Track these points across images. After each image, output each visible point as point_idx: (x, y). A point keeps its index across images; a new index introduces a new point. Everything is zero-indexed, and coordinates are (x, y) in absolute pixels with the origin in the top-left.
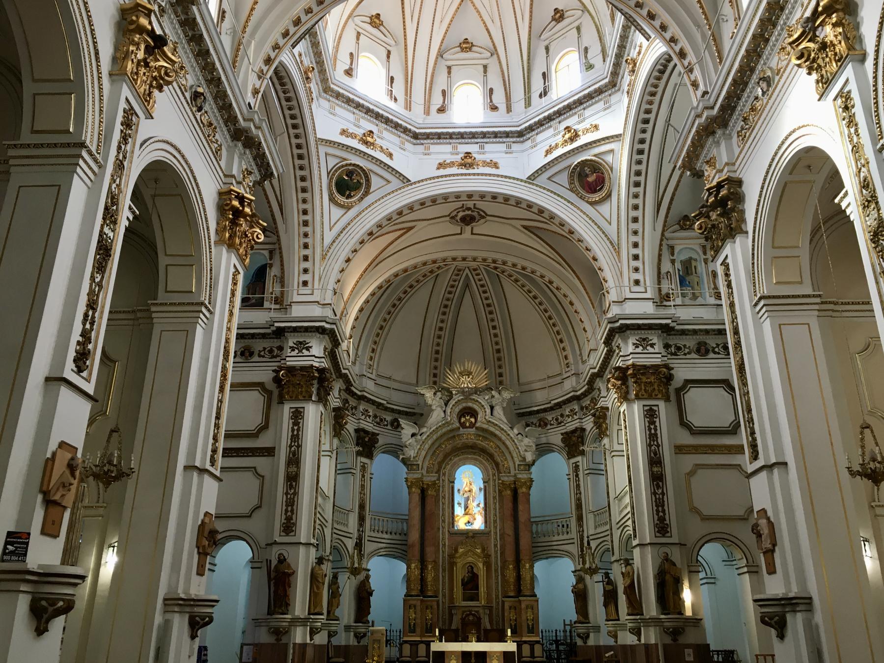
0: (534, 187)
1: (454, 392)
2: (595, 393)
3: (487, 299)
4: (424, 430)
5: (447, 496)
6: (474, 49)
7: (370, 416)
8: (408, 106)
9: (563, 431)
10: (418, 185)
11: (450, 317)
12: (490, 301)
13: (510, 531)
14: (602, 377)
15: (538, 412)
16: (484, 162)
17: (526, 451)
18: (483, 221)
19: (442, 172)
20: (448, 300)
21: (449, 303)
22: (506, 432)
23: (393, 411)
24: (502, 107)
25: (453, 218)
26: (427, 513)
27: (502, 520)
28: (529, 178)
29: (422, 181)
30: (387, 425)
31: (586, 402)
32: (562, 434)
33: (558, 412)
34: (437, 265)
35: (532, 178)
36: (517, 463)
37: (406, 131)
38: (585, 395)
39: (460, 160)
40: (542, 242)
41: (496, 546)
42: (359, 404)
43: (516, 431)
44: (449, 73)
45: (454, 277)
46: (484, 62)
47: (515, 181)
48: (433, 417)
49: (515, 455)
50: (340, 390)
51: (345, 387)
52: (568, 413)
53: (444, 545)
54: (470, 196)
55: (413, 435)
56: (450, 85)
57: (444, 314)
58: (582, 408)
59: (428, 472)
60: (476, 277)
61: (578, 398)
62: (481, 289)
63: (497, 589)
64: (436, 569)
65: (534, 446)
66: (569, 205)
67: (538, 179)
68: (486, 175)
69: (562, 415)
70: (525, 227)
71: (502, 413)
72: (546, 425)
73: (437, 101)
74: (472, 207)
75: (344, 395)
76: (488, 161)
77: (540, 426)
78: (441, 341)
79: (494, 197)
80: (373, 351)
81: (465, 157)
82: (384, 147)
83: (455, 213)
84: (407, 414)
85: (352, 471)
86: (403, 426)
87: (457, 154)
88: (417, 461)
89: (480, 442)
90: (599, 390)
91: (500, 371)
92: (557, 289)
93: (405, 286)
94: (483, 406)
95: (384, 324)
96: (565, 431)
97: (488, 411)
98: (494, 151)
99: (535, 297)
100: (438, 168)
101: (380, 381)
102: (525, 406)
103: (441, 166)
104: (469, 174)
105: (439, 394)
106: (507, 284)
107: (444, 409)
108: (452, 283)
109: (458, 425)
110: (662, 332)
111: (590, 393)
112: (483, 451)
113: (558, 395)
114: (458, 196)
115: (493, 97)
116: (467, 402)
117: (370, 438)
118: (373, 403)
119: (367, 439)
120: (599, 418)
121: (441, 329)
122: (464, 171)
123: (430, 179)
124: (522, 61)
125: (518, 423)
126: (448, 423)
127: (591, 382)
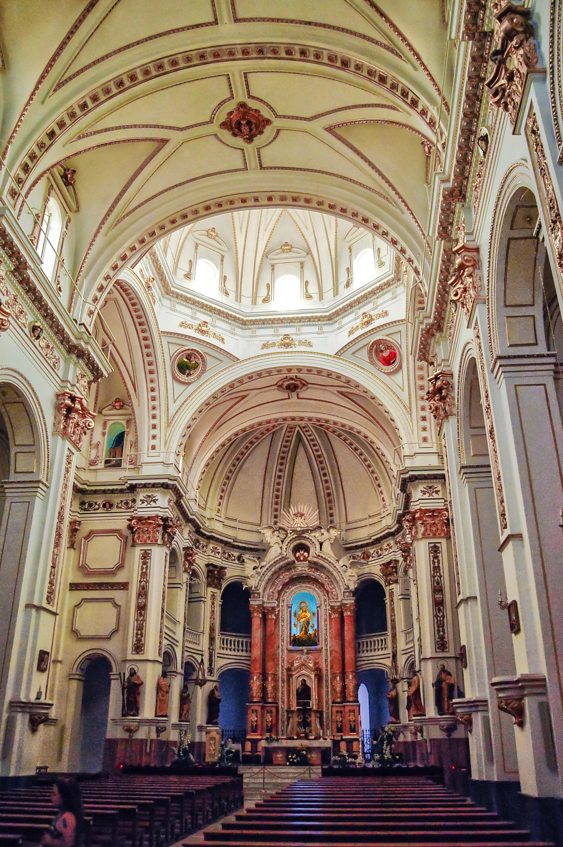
1: (289, 532)
3: (317, 451)
4: (263, 564)
5: (285, 619)
8: (238, 298)
9: (381, 563)
12: (319, 453)
15: (362, 546)
17: (349, 580)
18: (304, 388)
19: (266, 351)
20: (284, 452)
21: (285, 455)
25: (280, 386)
31: (399, 538)
37: (235, 319)
41: (326, 660)
49: (340, 583)
50: (190, 532)
51: (194, 530)
53: (283, 660)
54: (289, 370)
55: (254, 569)
56: (273, 280)
61: (392, 534)
63: (327, 695)
64: (275, 680)
69: (381, 549)
71: (329, 548)
73: (263, 292)
75: (195, 536)
77: (363, 558)
80: (221, 497)
81: (284, 338)
84: (251, 550)
85: (203, 599)
87: (278, 336)
91: (331, 511)
92: (371, 442)
93: (246, 443)
97: (318, 546)
99: (356, 449)
100: (262, 348)
101: (227, 522)
103: (265, 346)
105: (276, 532)
108: (286, 438)
109: (293, 559)
111: (401, 530)
112: (315, 581)
113: (375, 531)
114: (279, 371)
118: (221, 541)
119: (216, 573)
121: (280, 477)
122: (284, 350)
125: (344, 556)
126: (283, 558)
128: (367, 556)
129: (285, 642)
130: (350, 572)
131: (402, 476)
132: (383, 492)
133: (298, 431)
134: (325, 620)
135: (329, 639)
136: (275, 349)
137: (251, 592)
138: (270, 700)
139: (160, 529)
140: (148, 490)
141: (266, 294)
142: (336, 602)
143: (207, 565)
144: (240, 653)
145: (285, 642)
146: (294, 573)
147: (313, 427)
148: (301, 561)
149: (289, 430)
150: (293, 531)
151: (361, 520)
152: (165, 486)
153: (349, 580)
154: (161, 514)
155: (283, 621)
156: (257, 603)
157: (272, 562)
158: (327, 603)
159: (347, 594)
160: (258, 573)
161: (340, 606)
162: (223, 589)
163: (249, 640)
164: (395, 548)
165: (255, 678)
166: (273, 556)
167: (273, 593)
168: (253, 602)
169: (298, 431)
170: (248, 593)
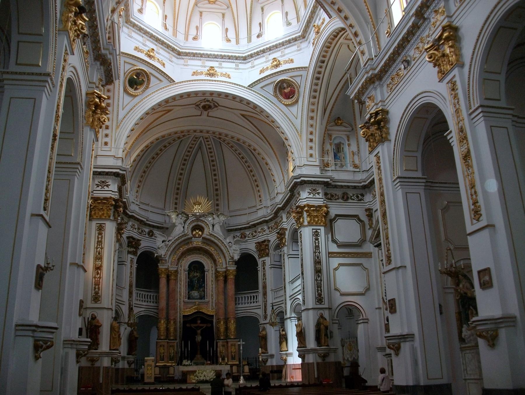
2: (278, 220)
3: (212, 157)
4: (170, 238)
5: (183, 279)
6: (217, 2)
7: (135, 229)
8: (175, 34)
10: (179, 84)
11: (188, 168)
12: (213, 158)
13: (222, 302)
14: (284, 210)
16: (222, 73)
17: (234, 253)
18: (216, 109)
20: (187, 156)
21: (188, 158)
22: (221, 241)
23: (150, 225)
24: (233, 41)
25: (197, 106)
26: (171, 290)
27: (218, 295)
28: (248, 86)
30: (145, 235)
31: (272, 224)
32: (256, 243)
34: (183, 134)
35: (251, 86)
36: (228, 260)
37: (173, 50)
38: (271, 220)
39: (206, 71)
42: (129, 221)
43: (228, 241)
44: (201, 16)
45: (192, 142)
46: (223, 11)
47: (240, 87)
48: (176, 230)
49: (226, 255)
52: (259, 231)
54: (212, 93)
55: (163, 242)
56: (201, 23)
57: (184, 165)
58: (269, 228)
59: (171, 264)
60: (206, 143)
61: (266, 222)
62: (209, 150)
66: (272, 105)
67: (254, 87)
68: (223, 82)
70: (243, 115)
72: (245, 237)
73: (193, 32)
76: (224, 73)
78: (181, 182)
79: (227, 95)
80: (139, 186)
81: (210, 69)
82: (160, 60)
84: (158, 228)
86: (157, 235)
87: (205, 67)
88: (165, 258)
89: (204, 247)
90: (281, 217)
91: (217, 202)
92: (259, 154)
95: (146, 170)
96: (257, 241)
97: (211, 228)
98: (228, 67)
99: (243, 158)
100: (193, 75)
102: (231, 226)
103: (194, 74)
105: (180, 215)
106: (226, 150)
107: (183, 225)
108: (191, 145)
109: (191, 236)
110: (324, 186)
113: (254, 218)
114: (204, 93)
115: (228, 34)
116: (198, 222)
117: (136, 242)
119: (134, 243)
120: (281, 234)
121: (181, 174)
122: (209, 78)
123: (187, 81)
124: (247, 14)
126: (185, 235)
127: (276, 214)
128: (243, 236)
129: (182, 296)
130: (234, 247)
131: (295, 180)
134: (212, 281)
135: (214, 295)
137: (160, 259)
138: (172, 338)
139: (112, 208)
140: (102, 176)
143: (128, 238)
144: (149, 304)
145: (182, 296)
146: (191, 246)
147: (213, 139)
148: (197, 237)
149: (194, 139)
150: (193, 215)
151: (239, 210)
152: (116, 175)
154: (113, 196)
155: (181, 281)
156: (164, 267)
157: (177, 237)
158: (214, 269)
159: (231, 263)
160: (166, 245)
161: (225, 272)
162: (138, 255)
163: (155, 295)
164: (267, 232)
165: (162, 322)
166: (178, 233)
167: (175, 260)
168: (161, 267)
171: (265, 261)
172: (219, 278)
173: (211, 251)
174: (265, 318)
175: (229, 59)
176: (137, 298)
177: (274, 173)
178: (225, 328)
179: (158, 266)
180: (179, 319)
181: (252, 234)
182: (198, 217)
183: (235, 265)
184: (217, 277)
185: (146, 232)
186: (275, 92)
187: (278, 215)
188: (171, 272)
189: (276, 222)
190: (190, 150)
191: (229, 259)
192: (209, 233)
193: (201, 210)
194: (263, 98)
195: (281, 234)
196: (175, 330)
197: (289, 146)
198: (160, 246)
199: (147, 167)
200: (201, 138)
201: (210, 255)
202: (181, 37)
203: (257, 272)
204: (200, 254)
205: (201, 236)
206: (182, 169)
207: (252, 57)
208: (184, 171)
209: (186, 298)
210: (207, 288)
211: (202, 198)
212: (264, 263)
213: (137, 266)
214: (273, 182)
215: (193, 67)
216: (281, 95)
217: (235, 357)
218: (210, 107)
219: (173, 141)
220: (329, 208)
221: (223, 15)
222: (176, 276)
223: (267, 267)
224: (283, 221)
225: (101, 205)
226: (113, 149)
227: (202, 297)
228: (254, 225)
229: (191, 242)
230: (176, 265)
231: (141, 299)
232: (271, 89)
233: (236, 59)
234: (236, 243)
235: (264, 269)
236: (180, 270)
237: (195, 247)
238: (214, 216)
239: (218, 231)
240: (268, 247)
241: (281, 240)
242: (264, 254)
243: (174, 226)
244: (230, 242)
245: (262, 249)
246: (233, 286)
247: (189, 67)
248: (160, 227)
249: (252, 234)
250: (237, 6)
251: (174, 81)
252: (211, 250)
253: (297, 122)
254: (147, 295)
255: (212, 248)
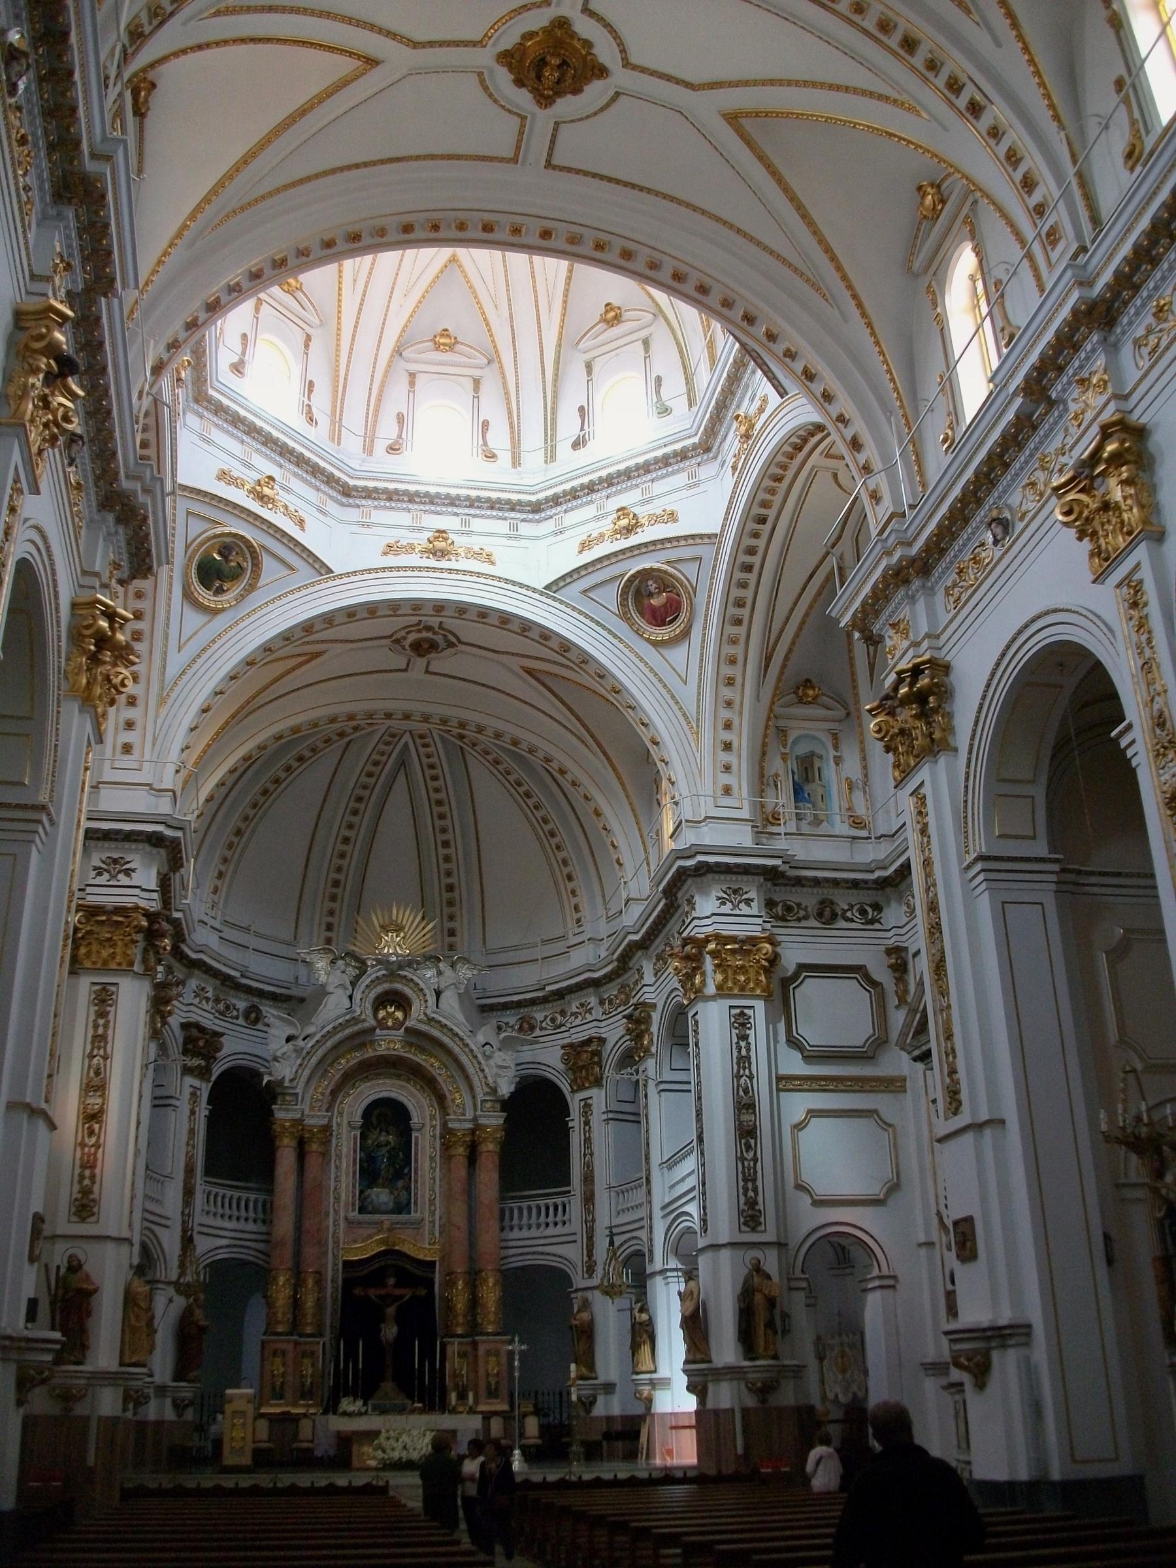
0: (556, 604)
2: (630, 977)
3: (437, 790)
4: (311, 1030)
5: (345, 1150)
6: (459, 347)
7: (208, 999)
10: (345, 580)
12: (442, 796)
14: (647, 948)
15: (519, 1004)
16: (469, 550)
17: (499, 1076)
18: (451, 651)
19: (391, 561)
20: (365, 787)
21: (367, 793)
22: (462, 1039)
23: (249, 990)
24: (505, 457)
25: (397, 641)
26: (308, 1185)
29: (355, 573)
30: (237, 1018)
31: (611, 990)
32: (563, 1047)
33: (558, 1005)
34: (355, 723)
36: (480, 1096)
38: (609, 978)
39: (425, 544)
40: (553, 698)
43: (481, 1038)
44: (412, 384)
45: (382, 747)
46: (477, 373)
47: (523, 591)
49: (476, 1082)
52: (574, 1010)
54: (439, 607)
55: (289, 1039)
56: (412, 405)
57: (355, 812)
58: (602, 1003)
59: (312, 1108)
60: (421, 750)
61: (596, 983)
62: (428, 772)
65: (513, 1066)
68: (472, 573)
69: (563, 1013)
70: (530, 672)
73: (387, 430)
74: (436, 626)
76: (476, 549)
78: (345, 863)
79: (483, 613)
80: (221, 875)
81: (436, 538)
83: (403, 633)
84: (274, 997)
86: (271, 1020)
87: (421, 529)
88: (295, 1088)
92: (574, 784)
93: (288, 758)
94: (422, 990)
95: (243, 826)
96: (568, 1041)
97: (431, 999)
99: (528, 795)
100: (385, 554)
103: (390, 549)
104: (442, 570)
105: (340, 962)
107: (349, 993)
108: (375, 757)
109: (373, 1023)
111: (619, 976)
114: (417, 605)
115: (488, 436)
116: (391, 982)
117: (207, 1041)
119: (201, 1043)
120: (638, 1022)
121: (346, 840)
122: (432, 563)
123: (369, 571)
124: (544, 382)
126: (355, 1021)
127: (625, 960)
128: (527, 1026)
129: (342, 1204)
131: (680, 863)
132: (578, 892)
133: (406, 744)
134: (432, 1159)
136: (414, 560)
137: (279, 1090)
138: (309, 1330)
139: (139, 937)
140: (113, 845)
141: (394, 436)
142: (460, 1120)
143: (185, 1026)
147: (441, 737)
148: (388, 1028)
149: (386, 738)
150: (379, 962)
151: (516, 948)
152: (155, 840)
153: (499, 1076)
154: (143, 904)
155: (339, 1157)
157: (329, 1028)
158: (437, 1123)
159: (489, 1105)
160: (298, 1051)
161: (473, 1132)
162: (213, 1078)
163: (262, 1197)
164: (598, 1013)
165: (281, 1280)
166: (333, 1015)
167: (323, 1094)
169: (406, 744)
170: (272, 1093)
171: (589, 1101)
172: (453, 1152)
173: (430, 1069)
174: (590, 1270)
175: (492, 508)
176: (206, 1208)
177: (620, 841)
178: (469, 1300)
179: (271, 1113)
180: (332, 1273)
181: (553, 1020)
182: (395, 967)
183: (502, 1111)
184: (446, 1147)
185: (237, 1010)
186: (623, 603)
187: (631, 964)
188: (310, 1131)
189: (623, 986)
190: (373, 769)
191: (486, 1094)
192: (425, 1014)
193: (401, 948)
194: (587, 622)
195: (638, 1022)
196: (320, 1302)
197: (663, 761)
198: (279, 1054)
199: (246, 819)
200: (407, 737)
201: (428, 1083)
202: (352, 444)
203: (565, 1131)
204: (398, 1077)
205: (402, 1023)
206: (350, 826)
207: (557, 504)
208: (355, 831)
209: (353, 1210)
210: (416, 1181)
211: (407, 913)
212: (587, 1107)
213: (211, 1111)
214: (617, 866)
215: (388, 531)
216: (642, 614)
217: (496, 1389)
218: (433, 646)
219: (326, 742)
220: (779, 943)
221: (477, 382)
222: (326, 1142)
223: (597, 1118)
224: (643, 982)
225: (106, 929)
226: (146, 765)
227: (402, 1207)
228: (560, 995)
229: (372, 1042)
230: (327, 1111)
231: (220, 1211)
232: (610, 596)
233: (512, 510)
234: (506, 1044)
235: (587, 1123)
236: (338, 1124)
237: (382, 1056)
238: (441, 965)
239: (452, 1009)
240: (600, 1059)
241: (639, 1037)
242: (587, 1079)
243: (322, 992)
244: (487, 1044)
245: (581, 1064)
246: (495, 1176)
247: (375, 530)
248: (281, 995)
249: (553, 1020)
250: (515, 357)
251: (330, 571)
252: (432, 1065)
253: (688, 694)
254: (239, 1199)
255: (432, 1060)
